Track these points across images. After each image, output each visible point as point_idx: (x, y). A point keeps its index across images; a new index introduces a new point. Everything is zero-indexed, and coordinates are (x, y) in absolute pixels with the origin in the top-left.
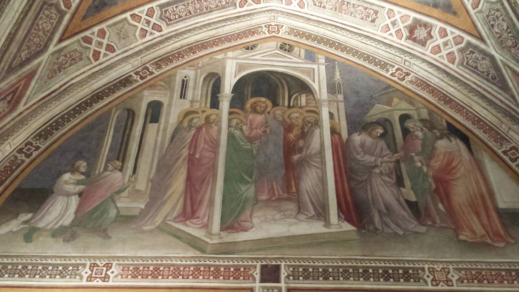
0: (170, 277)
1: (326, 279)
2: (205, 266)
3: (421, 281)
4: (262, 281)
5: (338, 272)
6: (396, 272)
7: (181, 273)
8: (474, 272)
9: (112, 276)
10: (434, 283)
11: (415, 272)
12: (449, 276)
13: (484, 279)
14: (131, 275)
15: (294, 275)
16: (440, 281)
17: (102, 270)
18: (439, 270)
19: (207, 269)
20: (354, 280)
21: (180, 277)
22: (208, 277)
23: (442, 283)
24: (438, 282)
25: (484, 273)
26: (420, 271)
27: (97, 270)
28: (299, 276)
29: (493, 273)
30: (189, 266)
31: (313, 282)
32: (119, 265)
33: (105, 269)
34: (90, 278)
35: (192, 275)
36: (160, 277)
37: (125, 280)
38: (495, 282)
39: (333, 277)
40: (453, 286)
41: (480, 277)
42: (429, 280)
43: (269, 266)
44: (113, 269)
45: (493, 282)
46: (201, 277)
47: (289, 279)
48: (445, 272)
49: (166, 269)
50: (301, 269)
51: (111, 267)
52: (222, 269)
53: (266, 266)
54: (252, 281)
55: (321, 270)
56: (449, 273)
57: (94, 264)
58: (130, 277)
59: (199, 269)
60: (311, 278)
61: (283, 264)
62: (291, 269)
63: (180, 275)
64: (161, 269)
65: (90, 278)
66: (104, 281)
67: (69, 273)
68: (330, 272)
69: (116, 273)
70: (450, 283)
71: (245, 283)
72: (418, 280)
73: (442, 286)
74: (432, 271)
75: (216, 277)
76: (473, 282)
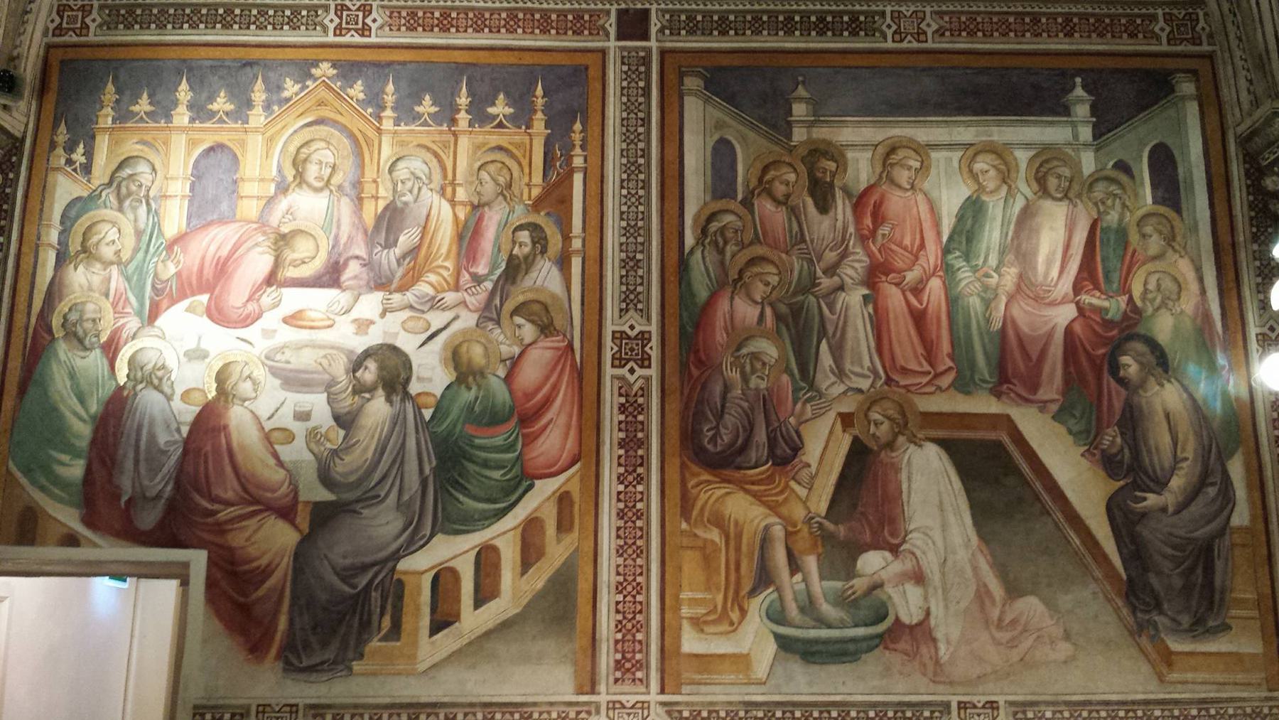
0: (470, 30)
1: (723, 33)
2: (525, 11)
3: (877, 34)
4: (620, 37)
5: (744, 22)
6: (837, 19)
7: (487, 22)
8: (963, 19)
9: (374, 26)
10: (897, 37)
11: (869, 19)
12: (923, 26)
13: (979, 30)
14: (404, 25)
15: (672, 27)
16: (907, 34)
17: (357, 16)
18: (908, 14)
19: (528, 16)
20: (769, 34)
21: (486, 30)
22: (530, 30)
23: (909, 37)
24: (903, 35)
25: (979, 19)
26: (877, 18)
27: (348, 15)
28: (679, 29)
29: (995, 20)
30: (500, 10)
31: (702, 38)
32: (383, 7)
33: (361, 14)
34: (339, 31)
35: (505, 26)
36: (453, 30)
37: (395, 33)
38: (996, 34)
39: (736, 30)
40: (926, 41)
41: (972, 26)
42: (889, 33)
43: (631, 12)
44: (374, 15)
45: (992, 35)
46: (520, 31)
47: (664, 34)
48: (917, 18)
49: (462, 15)
50: (683, 17)
51: (370, 12)
52: (554, 17)
53: (627, 11)
54: (604, 38)
55: (716, 18)
56: (923, 19)
57: (342, 5)
58: (403, 28)
59: (517, 16)
60: (699, 32)
61: (654, 7)
62: (667, 17)
63: (486, 26)
64: (454, 15)
65: (339, 31)
66: (363, 35)
67: (304, 20)
68: (731, 22)
69: (380, 21)
70: (922, 37)
71: (593, 41)
72: (871, 32)
73: (910, 42)
74: (897, 16)
75: (545, 31)
76: (960, 35)
